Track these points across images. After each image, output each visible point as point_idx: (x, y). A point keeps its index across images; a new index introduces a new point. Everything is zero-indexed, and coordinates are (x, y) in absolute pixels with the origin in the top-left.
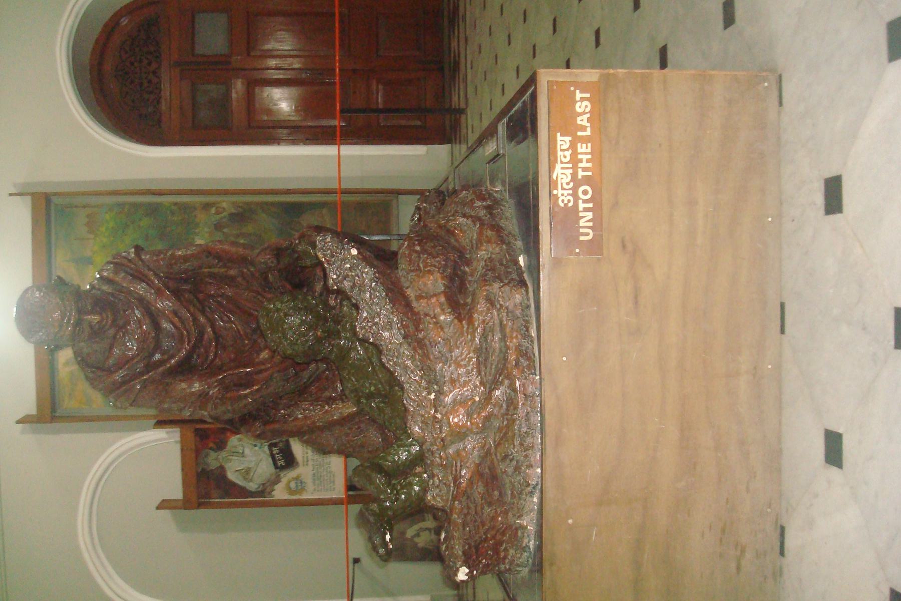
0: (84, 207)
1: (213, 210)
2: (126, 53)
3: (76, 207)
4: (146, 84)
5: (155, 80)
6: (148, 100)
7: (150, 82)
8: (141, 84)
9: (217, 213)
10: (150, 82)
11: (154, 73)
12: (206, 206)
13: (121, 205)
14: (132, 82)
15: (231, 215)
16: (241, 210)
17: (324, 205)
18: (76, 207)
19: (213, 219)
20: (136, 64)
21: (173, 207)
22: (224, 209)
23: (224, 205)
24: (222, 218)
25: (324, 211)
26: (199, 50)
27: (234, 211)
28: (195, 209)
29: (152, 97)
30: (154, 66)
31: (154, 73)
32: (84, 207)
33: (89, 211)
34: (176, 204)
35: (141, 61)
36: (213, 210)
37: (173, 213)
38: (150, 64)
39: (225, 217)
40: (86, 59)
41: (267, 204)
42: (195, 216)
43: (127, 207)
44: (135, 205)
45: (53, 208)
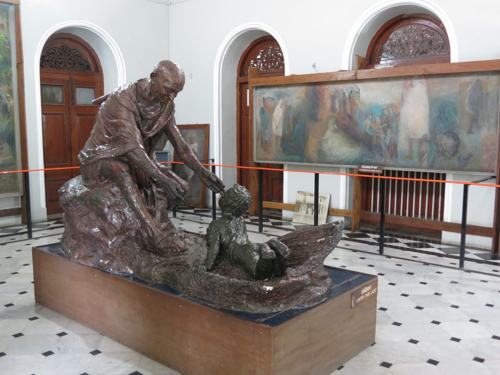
0: (8, 23)
1: (8, 95)
2: (74, 53)
3: (7, 18)
4: (60, 61)
5: (62, 65)
6: (52, 61)
7: (61, 63)
8: (59, 58)
9: (7, 97)
10: (61, 63)
11: (65, 66)
12: (11, 92)
13: (9, 44)
14: (61, 54)
15: (7, 105)
16: (9, 110)
17: (14, 155)
18: (7, 18)
19: (4, 95)
20: (69, 57)
21: (9, 73)
22: (10, 101)
23: (12, 102)
24: (4, 99)
25: (11, 156)
26: (78, 90)
27: (9, 106)
28: (9, 85)
29: (54, 64)
30: (69, 66)
31: (65, 66)
32: (8, 23)
33: (5, 25)
34: (11, 75)
35: (71, 59)
36: (8, 95)
37: (6, 73)
38: (69, 64)
39: (5, 101)
40: (74, 33)
41: (13, 126)
42: (4, 85)
43: (9, 47)
44: (9, 52)
45: (8, 5)
